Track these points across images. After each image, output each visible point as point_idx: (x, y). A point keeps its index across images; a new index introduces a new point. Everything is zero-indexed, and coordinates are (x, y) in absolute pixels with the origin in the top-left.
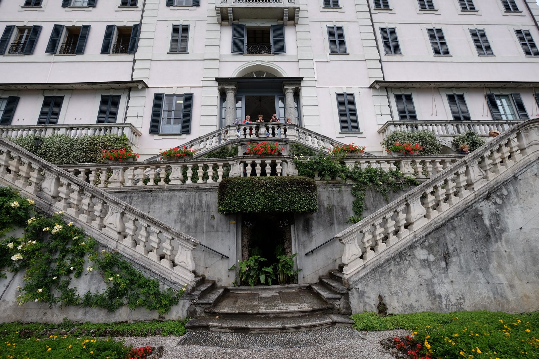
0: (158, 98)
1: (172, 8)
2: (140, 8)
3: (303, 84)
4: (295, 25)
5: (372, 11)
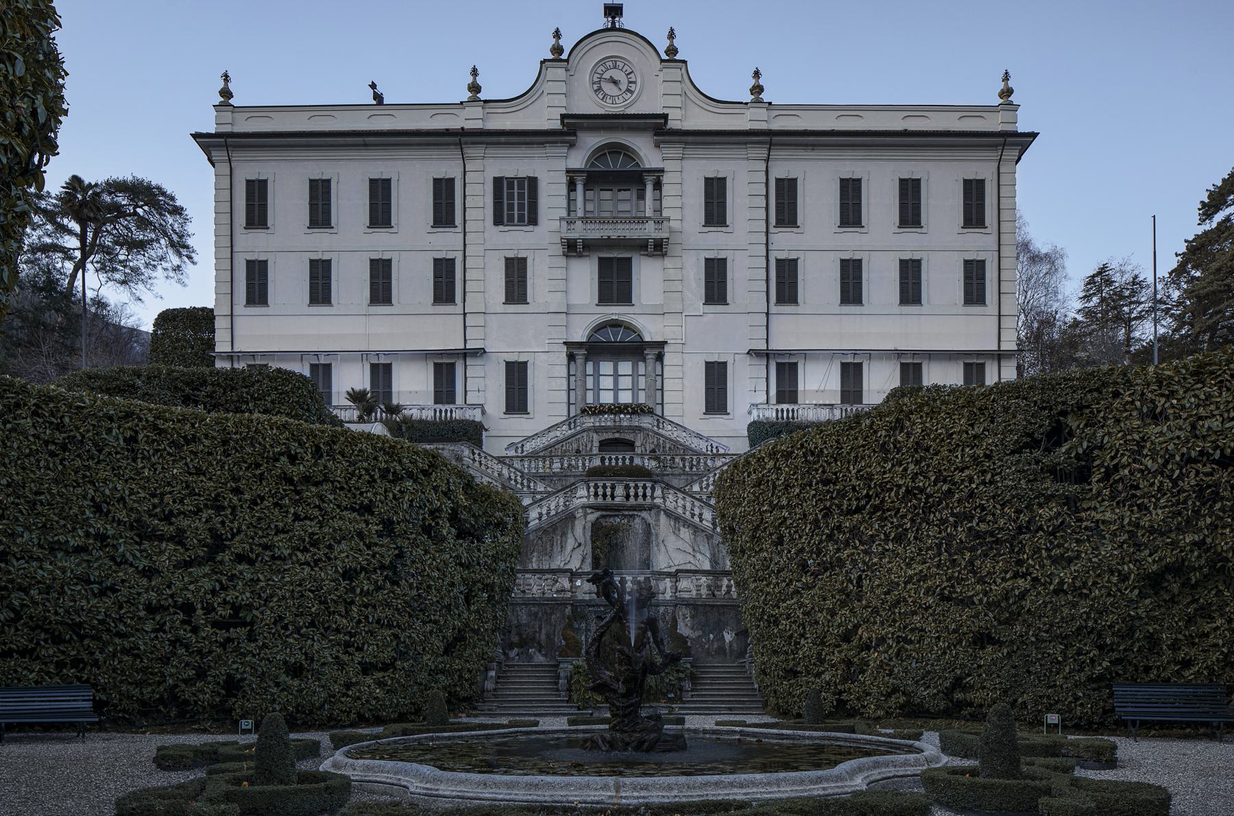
1: (501, 228)
2: (460, 229)
3: (667, 348)
5: (772, 230)
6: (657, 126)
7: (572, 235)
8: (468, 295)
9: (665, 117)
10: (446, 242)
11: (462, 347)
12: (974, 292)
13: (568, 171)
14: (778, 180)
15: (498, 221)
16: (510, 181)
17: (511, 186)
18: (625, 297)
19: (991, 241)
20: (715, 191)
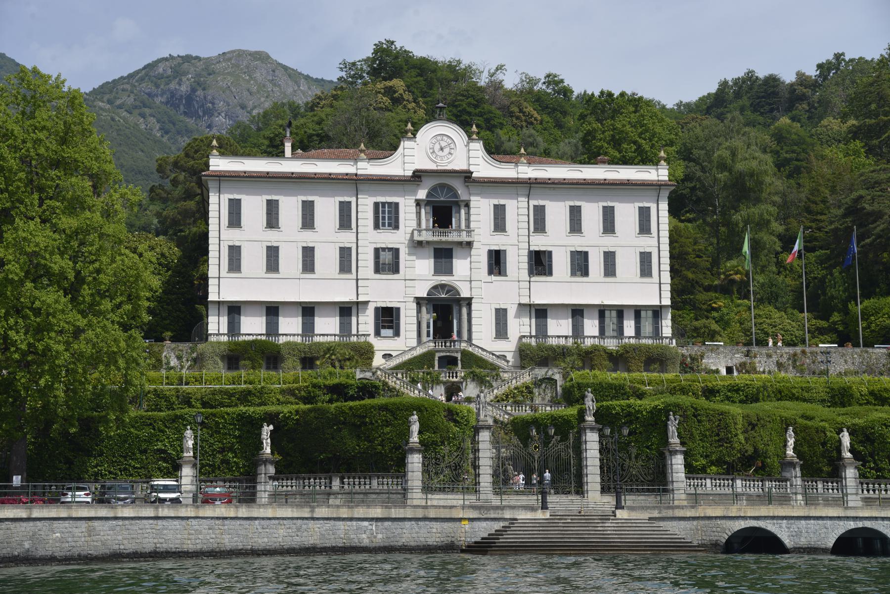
0: (377, 309)
1: (379, 231)
2: (354, 230)
4: (471, 248)
5: (531, 234)
6: (466, 176)
7: (420, 239)
9: (472, 173)
10: (347, 238)
11: (356, 300)
13: (416, 200)
14: (535, 206)
15: (376, 226)
16: (384, 204)
18: (449, 271)
20: (499, 213)
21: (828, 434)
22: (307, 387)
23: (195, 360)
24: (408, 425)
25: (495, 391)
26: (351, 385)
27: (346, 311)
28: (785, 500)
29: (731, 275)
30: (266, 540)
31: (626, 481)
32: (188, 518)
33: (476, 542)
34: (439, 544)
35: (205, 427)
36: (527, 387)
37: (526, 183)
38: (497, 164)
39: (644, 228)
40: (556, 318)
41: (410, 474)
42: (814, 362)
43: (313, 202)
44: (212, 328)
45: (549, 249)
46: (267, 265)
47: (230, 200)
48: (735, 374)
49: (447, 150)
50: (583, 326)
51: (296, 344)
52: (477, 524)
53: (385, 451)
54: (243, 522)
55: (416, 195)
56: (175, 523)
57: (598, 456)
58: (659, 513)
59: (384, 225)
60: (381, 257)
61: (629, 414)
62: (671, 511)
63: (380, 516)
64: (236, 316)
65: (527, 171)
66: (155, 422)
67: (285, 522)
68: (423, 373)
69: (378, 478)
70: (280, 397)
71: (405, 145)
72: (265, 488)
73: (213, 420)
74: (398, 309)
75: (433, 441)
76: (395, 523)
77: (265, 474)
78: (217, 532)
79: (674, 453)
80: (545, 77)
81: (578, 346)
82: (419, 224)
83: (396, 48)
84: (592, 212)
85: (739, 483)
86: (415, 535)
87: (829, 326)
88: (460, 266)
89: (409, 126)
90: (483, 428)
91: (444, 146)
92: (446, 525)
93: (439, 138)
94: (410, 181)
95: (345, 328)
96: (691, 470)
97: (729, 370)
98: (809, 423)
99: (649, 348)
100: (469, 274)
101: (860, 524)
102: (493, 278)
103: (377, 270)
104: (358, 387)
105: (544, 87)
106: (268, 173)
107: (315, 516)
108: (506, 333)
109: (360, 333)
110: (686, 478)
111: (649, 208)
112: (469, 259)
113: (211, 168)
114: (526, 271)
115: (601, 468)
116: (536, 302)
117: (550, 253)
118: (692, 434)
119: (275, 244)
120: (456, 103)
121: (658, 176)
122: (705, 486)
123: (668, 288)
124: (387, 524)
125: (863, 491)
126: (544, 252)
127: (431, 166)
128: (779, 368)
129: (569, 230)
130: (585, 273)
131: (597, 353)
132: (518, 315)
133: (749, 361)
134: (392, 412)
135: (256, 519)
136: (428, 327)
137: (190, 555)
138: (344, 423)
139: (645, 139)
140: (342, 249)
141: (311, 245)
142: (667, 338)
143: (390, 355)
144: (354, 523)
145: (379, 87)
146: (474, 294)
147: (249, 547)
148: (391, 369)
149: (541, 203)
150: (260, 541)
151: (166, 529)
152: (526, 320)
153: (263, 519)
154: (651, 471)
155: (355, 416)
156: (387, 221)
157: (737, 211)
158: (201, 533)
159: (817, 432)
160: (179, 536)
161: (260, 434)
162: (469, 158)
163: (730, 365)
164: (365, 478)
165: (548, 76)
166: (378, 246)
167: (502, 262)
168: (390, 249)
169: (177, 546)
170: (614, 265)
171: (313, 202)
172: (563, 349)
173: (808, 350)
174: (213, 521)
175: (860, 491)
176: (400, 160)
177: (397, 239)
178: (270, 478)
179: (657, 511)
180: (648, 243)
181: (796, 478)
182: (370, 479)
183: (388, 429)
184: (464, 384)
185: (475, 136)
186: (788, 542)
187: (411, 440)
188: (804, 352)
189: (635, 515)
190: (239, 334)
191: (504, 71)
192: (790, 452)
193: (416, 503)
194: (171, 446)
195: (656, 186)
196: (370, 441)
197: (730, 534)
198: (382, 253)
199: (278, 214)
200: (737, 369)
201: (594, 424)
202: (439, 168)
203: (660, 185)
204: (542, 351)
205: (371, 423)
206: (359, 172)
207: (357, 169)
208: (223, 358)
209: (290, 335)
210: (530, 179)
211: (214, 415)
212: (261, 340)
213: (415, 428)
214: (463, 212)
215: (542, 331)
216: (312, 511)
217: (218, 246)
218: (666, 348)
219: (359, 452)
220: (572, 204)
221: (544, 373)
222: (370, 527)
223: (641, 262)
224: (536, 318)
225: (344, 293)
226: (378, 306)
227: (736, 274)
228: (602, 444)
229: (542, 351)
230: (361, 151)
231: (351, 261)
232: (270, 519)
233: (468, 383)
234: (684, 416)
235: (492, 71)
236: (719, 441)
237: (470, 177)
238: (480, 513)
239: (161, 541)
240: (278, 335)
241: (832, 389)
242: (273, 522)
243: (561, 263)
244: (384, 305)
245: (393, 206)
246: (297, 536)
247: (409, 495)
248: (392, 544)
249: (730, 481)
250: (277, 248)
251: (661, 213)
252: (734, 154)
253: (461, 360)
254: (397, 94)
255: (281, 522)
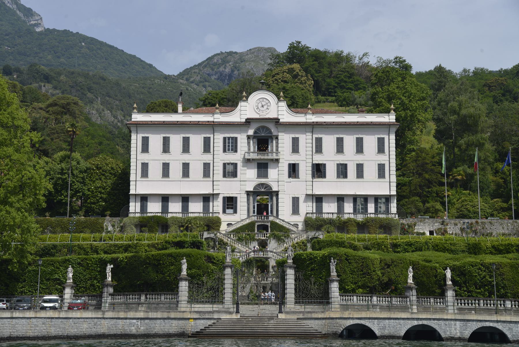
0: (224, 198)
1: (226, 153)
2: (212, 153)
4: (279, 162)
5: (314, 154)
6: (276, 121)
8: (214, 175)
10: (208, 158)
11: (212, 193)
12: (381, 173)
13: (247, 136)
14: (316, 138)
15: (224, 151)
16: (229, 138)
17: (229, 139)
18: (266, 176)
19: (387, 158)
20: (295, 142)
21: (438, 271)
22: (163, 242)
23: (122, 227)
24: (181, 264)
25: (285, 245)
26: (187, 242)
27: (206, 199)
28: (405, 309)
29: (456, 176)
30: (76, 330)
31: (309, 297)
32: (30, 318)
33: (197, 332)
34: (176, 333)
35: (81, 266)
36: (303, 243)
37: (311, 125)
38: (294, 114)
39: (381, 149)
40: (328, 202)
41: (180, 293)
42: (483, 228)
43: (189, 138)
44: (132, 209)
45: (324, 162)
46: (163, 174)
47: (143, 137)
48: (435, 235)
49: (265, 107)
50: (344, 207)
51: (177, 218)
52: (198, 322)
53: (171, 279)
54: (63, 320)
55: (247, 133)
56: (23, 321)
57: (294, 282)
58: (303, 315)
59: (229, 150)
60: (227, 168)
61: (311, 259)
62: (310, 314)
63: (143, 317)
64: (145, 202)
65: (312, 118)
66: (55, 263)
67: (88, 320)
68: (246, 234)
69: (165, 295)
70: (147, 248)
71: (242, 104)
72: (107, 300)
73: (86, 262)
74: (236, 198)
75: (198, 274)
76: (151, 321)
77: (107, 292)
78: (48, 326)
79: (333, 281)
80: (394, 59)
81: (340, 218)
82: (249, 149)
83: (302, 45)
84: (350, 141)
85: (375, 298)
86: (162, 328)
87: (508, 207)
88: (272, 173)
89: (244, 94)
90: (227, 267)
91: (264, 104)
92: (181, 322)
93: (261, 100)
94: (243, 125)
95: (206, 209)
96: (343, 290)
97: (431, 233)
98: (427, 264)
99: (381, 220)
100: (277, 177)
101: (420, 323)
102: (291, 179)
103: (224, 176)
104: (190, 243)
105: (394, 65)
106: (164, 122)
107: (105, 317)
108: (298, 211)
109: (214, 211)
110: (340, 295)
111: (384, 138)
112: (277, 169)
113: (133, 120)
114: (311, 175)
115: (295, 289)
116: (317, 193)
117: (325, 165)
118: (345, 270)
119: (167, 162)
120: (338, 76)
121: (389, 119)
122: (353, 300)
123: (395, 184)
124: (146, 321)
125: (458, 304)
126: (321, 164)
127: (257, 116)
128: (461, 231)
129: (355, 152)
130: (345, 176)
131: (350, 222)
132: (305, 201)
133: (443, 228)
134: (174, 257)
135: (70, 318)
136: (254, 208)
137: (30, 339)
138: (149, 264)
139: (405, 97)
140: (205, 164)
141: (187, 162)
142: (393, 214)
143: (231, 224)
144: (128, 321)
145: (285, 68)
146: (280, 189)
147: (66, 334)
148: (230, 232)
149: (320, 136)
150: (72, 331)
151: (18, 324)
152: (310, 204)
153: (75, 318)
154: (321, 292)
155: (154, 260)
156: (230, 148)
157: (462, 138)
158: (38, 326)
159: (431, 269)
160: (25, 328)
161: (106, 270)
162: (278, 111)
163: (432, 230)
164: (158, 295)
165: (396, 58)
166: (225, 162)
167: (296, 170)
168: (232, 164)
169: (23, 334)
170: (362, 171)
171: (189, 138)
172: (330, 220)
173: (479, 221)
174: (45, 320)
175: (456, 304)
176: (238, 113)
177: (236, 158)
178: (110, 294)
179: (301, 315)
180: (383, 159)
181: (413, 295)
182: (160, 295)
183: (172, 267)
184: (269, 241)
185: (282, 99)
186: (377, 333)
187: (182, 273)
188: (477, 222)
189: (289, 317)
190: (147, 213)
191: (368, 56)
192: (410, 281)
193: (183, 309)
194: (63, 276)
195: (388, 125)
196: (163, 274)
197: (344, 328)
198: (227, 166)
199: (169, 145)
200: (436, 232)
201: (292, 264)
202: (261, 117)
203: (390, 125)
204: (318, 222)
205: (163, 264)
206: (215, 120)
207: (214, 119)
208: (136, 226)
209: (174, 213)
210: (313, 122)
211: (86, 259)
212: (157, 216)
213: (185, 267)
214: (274, 142)
215: (319, 210)
216: (103, 314)
217: (135, 163)
218: (392, 219)
219: (157, 280)
220: (338, 136)
221: (313, 234)
222: (137, 323)
223: (378, 169)
224: (316, 202)
225: (205, 189)
226: (225, 196)
227: (459, 176)
228: (297, 276)
229: (318, 222)
230: (217, 108)
231: (209, 171)
232: (79, 318)
233: (271, 240)
234: (340, 260)
235: (361, 57)
236: (363, 274)
237: (278, 122)
238: (200, 315)
239: (14, 331)
240: (167, 212)
241: (469, 244)
242: (81, 320)
243: (331, 171)
244: (228, 196)
245: (234, 139)
246: (94, 328)
247: (179, 305)
248: (149, 332)
249: (369, 298)
250: (168, 164)
251: (391, 141)
252: (460, 105)
253: (270, 227)
254: (295, 72)
255: (85, 320)
